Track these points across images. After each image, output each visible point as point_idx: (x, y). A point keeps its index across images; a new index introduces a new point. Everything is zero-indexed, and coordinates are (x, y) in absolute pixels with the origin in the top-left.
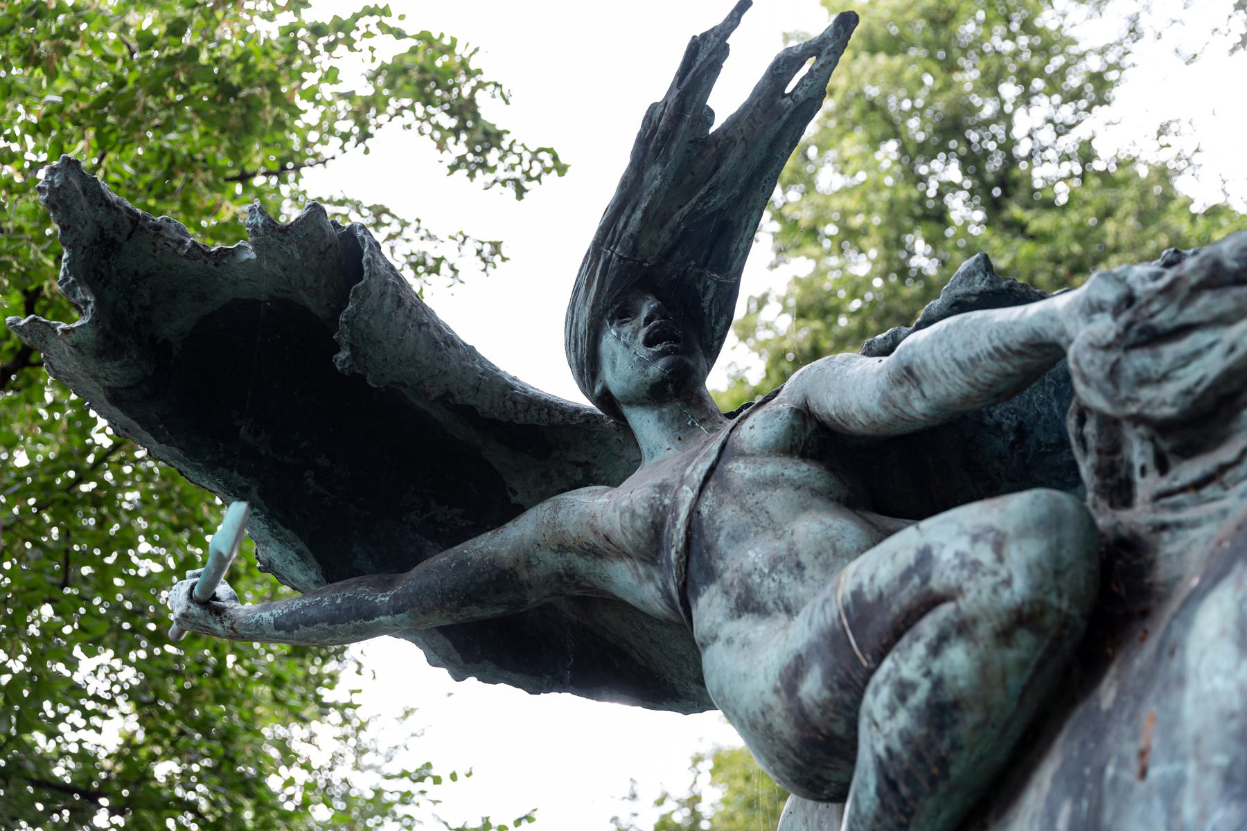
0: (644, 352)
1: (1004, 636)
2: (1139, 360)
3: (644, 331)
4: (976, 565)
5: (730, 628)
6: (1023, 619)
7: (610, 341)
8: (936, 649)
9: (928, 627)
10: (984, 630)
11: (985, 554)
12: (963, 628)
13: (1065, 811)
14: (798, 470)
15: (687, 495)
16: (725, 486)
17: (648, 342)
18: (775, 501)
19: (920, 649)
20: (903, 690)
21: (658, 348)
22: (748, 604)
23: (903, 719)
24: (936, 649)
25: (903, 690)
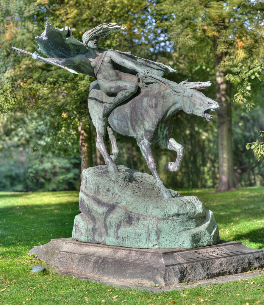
0: (94, 45)
1: (131, 93)
2: (144, 78)
3: (94, 43)
4: (130, 89)
5: (103, 79)
6: (132, 93)
7: (90, 42)
8: (126, 93)
9: (126, 91)
10: (130, 93)
11: (131, 88)
12: (128, 92)
13: (132, 105)
14: (110, 65)
15: (99, 65)
16: (103, 65)
17: (95, 44)
18: (108, 68)
19: (125, 92)
20: (123, 95)
21: (95, 45)
22: (105, 78)
23: (122, 96)
24: (126, 93)
25: (123, 95)
